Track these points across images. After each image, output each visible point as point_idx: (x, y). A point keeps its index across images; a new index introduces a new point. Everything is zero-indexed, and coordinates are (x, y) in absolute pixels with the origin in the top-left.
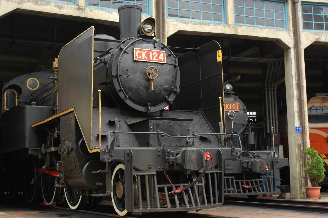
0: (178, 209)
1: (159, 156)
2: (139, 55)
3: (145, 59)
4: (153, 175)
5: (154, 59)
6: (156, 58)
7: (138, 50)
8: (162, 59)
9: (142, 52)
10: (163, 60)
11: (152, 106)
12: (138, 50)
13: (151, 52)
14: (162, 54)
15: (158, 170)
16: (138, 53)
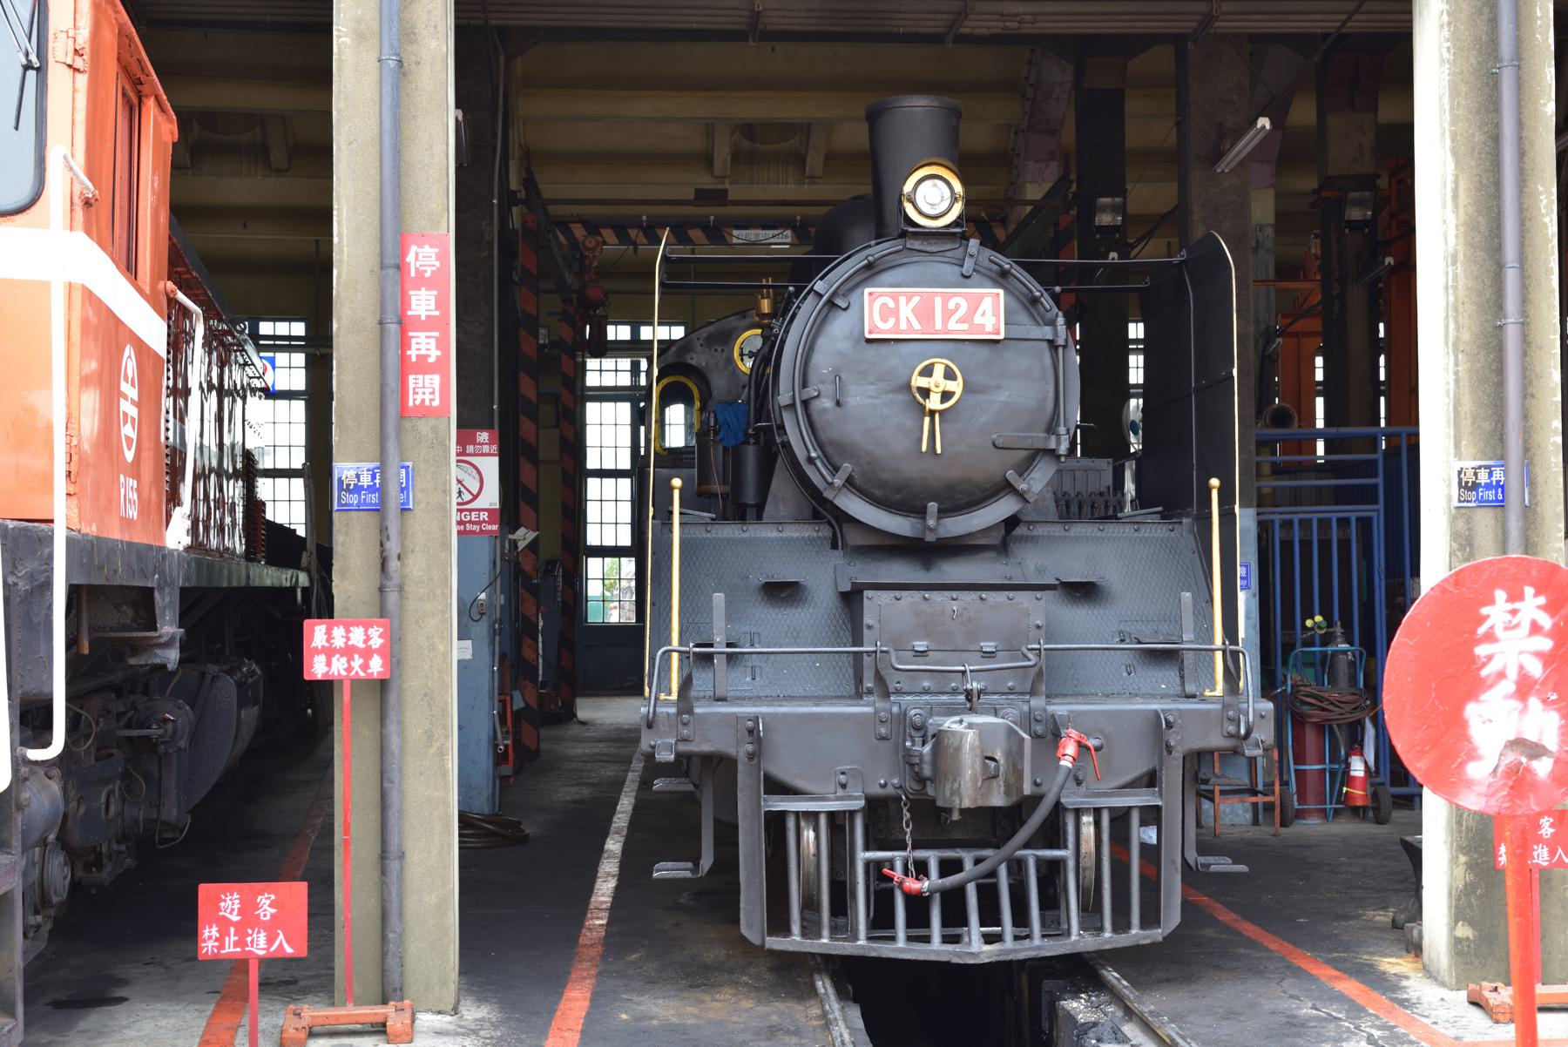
0: (937, 952)
1: (883, 738)
2: (886, 313)
4: (852, 813)
5: (952, 325)
6: (960, 321)
10: (989, 328)
11: (943, 512)
12: (881, 295)
13: (938, 301)
14: (987, 304)
15: (876, 790)
16: (884, 305)
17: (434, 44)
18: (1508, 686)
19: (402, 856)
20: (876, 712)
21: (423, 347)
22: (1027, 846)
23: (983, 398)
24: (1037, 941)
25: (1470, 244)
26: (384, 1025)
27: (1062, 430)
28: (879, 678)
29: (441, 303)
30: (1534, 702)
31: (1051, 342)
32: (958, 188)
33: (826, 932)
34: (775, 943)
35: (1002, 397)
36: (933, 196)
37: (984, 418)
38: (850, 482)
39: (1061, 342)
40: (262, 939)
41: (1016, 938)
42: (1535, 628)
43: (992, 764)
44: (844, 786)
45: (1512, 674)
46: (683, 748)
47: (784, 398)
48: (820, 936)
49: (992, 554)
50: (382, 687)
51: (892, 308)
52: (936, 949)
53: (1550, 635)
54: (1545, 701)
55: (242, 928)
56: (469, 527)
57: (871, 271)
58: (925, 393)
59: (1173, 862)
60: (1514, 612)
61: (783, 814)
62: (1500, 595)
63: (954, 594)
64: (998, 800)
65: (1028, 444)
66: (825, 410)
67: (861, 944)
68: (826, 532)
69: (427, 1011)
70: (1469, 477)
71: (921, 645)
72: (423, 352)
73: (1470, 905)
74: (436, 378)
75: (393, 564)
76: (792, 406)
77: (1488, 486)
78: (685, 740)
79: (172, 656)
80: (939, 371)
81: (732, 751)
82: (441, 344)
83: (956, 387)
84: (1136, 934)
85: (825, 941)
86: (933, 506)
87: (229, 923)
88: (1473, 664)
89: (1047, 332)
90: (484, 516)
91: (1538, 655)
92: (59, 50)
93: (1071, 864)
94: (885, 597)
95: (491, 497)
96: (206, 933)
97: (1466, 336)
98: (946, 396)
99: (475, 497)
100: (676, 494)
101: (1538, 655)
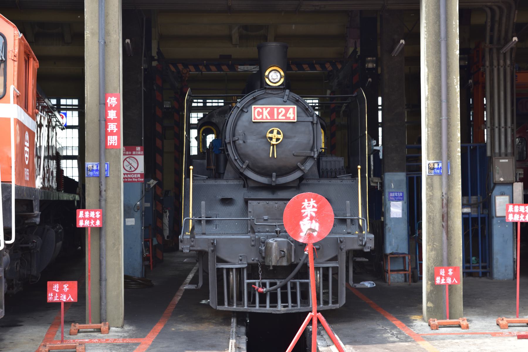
0: (268, 310)
1: (253, 246)
2: (259, 113)
3: (267, 119)
4: (243, 268)
6: (283, 116)
8: (292, 116)
9: (263, 110)
10: (292, 118)
11: (278, 176)
13: (276, 110)
14: (291, 111)
15: (251, 262)
16: (258, 111)
17: (115, 36)
18: (308, 218)
19: (106, 280)
20: (251, 238)
21: (112, 127)
22: (296, 277)
23: (290, 140)
24: (299, 307)
25: (432, 94)
26: (100, 329)
27: (315, 150)
28: (252, 228)
29: (118, 114)
30: (314, 221)
31: (312, 122)
32: (282, 73)
33: (235, 304)
34: (220, 308)
35: (296, 140)
36: (275, 77)
38: (248, 167)
39: (315, 122)
40: (65, 297)
41: (292, 306)
42: (313, 207)
43: (283, 253)
44: (241, 260)
45: (309, 216)
46: (191, 248)
47: (227, 141)
48: (233, 306)
49: (294, 189)
50: (100, 229)
51: (260, 112)
52: (268, 309)
53: (316, 208)
54: (316, 221)
55: (59, 294)
56: (134, 180)
57: (255, 101)
58: (271, 139)
59: (343, 284)
60: (309, 204)
61: (223, 268)
62: (306, 200)
63: (276, 202)
64: (284, 263)
65: (304, 154)
66: (240, 144)
67: (246, 308)
68: (242, 182)
69: (114, 327)
70: (432, 166)
71: (266, 217)
72: (112, 129)
73: (432, 297)
74: (116, 137)
75: (103, 193)
76: (230, 143)
77: (438, 169)
78: (192, 246)
79: (38, 220)
80: (275, 132)
81: (207, 250)
82: (118, 127)
83: (281, 137)
86: (274, 174)
87: (56, 292)
88: (301, 214)
89: (310, 119)
90: (139, 176)
91: (314, 212)
92: (10, 55)
94: (255, 203)
95: (141, 169)
96: (49, 295)
97: (431, 122)
98: (278, 140)
99: (136, 169)
100: (191, 171)
101: (314, 212)
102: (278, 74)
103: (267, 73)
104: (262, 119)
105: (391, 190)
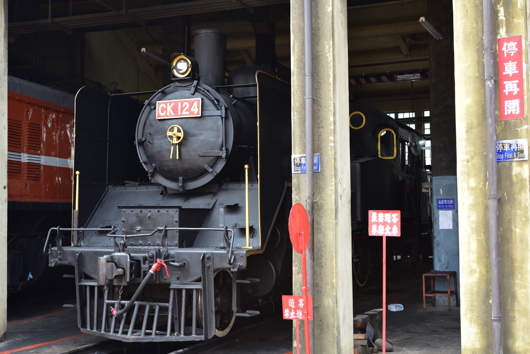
0: (119, 337)
7: (162, 103)
9: (167, 106)
10: (196, 113)
12: (162, 103)
13: (180, 104)
14: (195, 104)
23: (195, 138)
24: (153, 336)
32: (190, 62)
35: (202, 137)
36: (182, 67)
37: (195, 146)
57: (164, 94)
59: (212, 311)
61: (86, 286)
63: (149, 210)
71: (138, 228)
80: (176, 129)
83: (181, 135)
84: (194, 337)
85: (103, 332)
89: (218, 113)
93: (170, 308)
98: (179, 138)
102: (186, 64)
103: (174, 64)
104: (166, 115)
105: (439, 197)
